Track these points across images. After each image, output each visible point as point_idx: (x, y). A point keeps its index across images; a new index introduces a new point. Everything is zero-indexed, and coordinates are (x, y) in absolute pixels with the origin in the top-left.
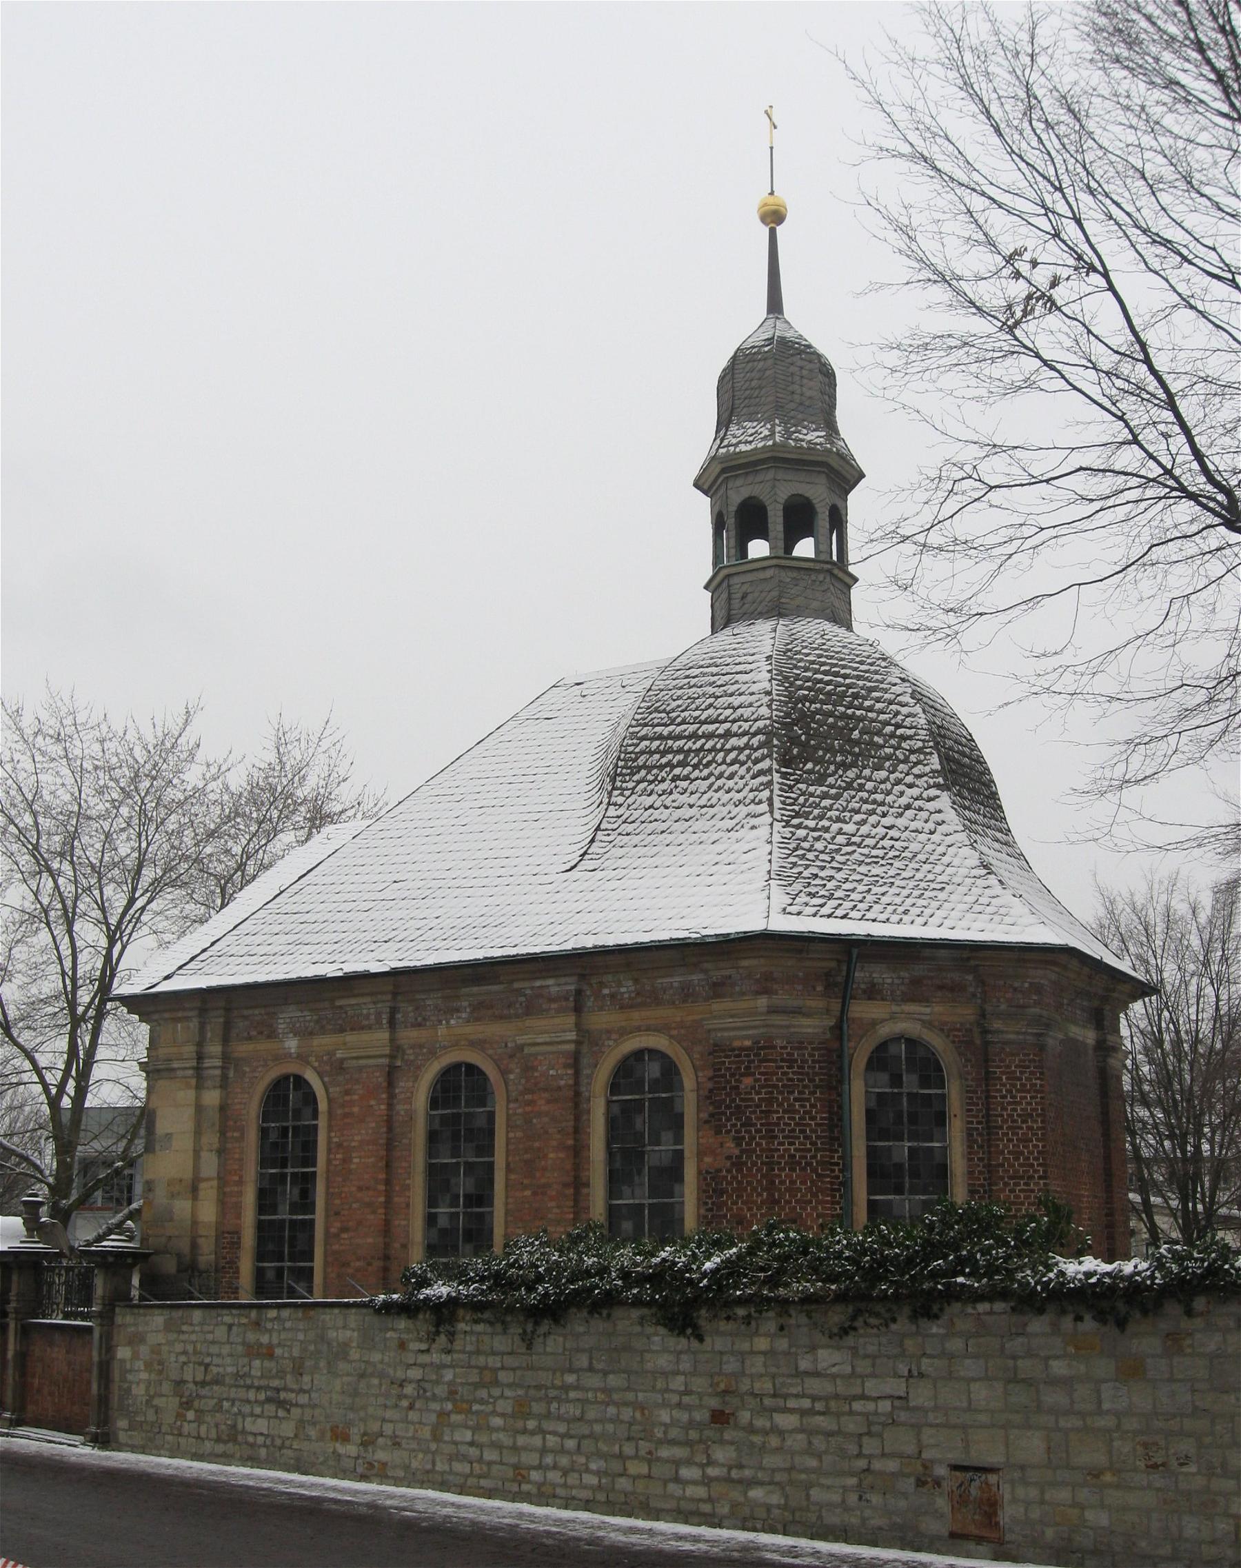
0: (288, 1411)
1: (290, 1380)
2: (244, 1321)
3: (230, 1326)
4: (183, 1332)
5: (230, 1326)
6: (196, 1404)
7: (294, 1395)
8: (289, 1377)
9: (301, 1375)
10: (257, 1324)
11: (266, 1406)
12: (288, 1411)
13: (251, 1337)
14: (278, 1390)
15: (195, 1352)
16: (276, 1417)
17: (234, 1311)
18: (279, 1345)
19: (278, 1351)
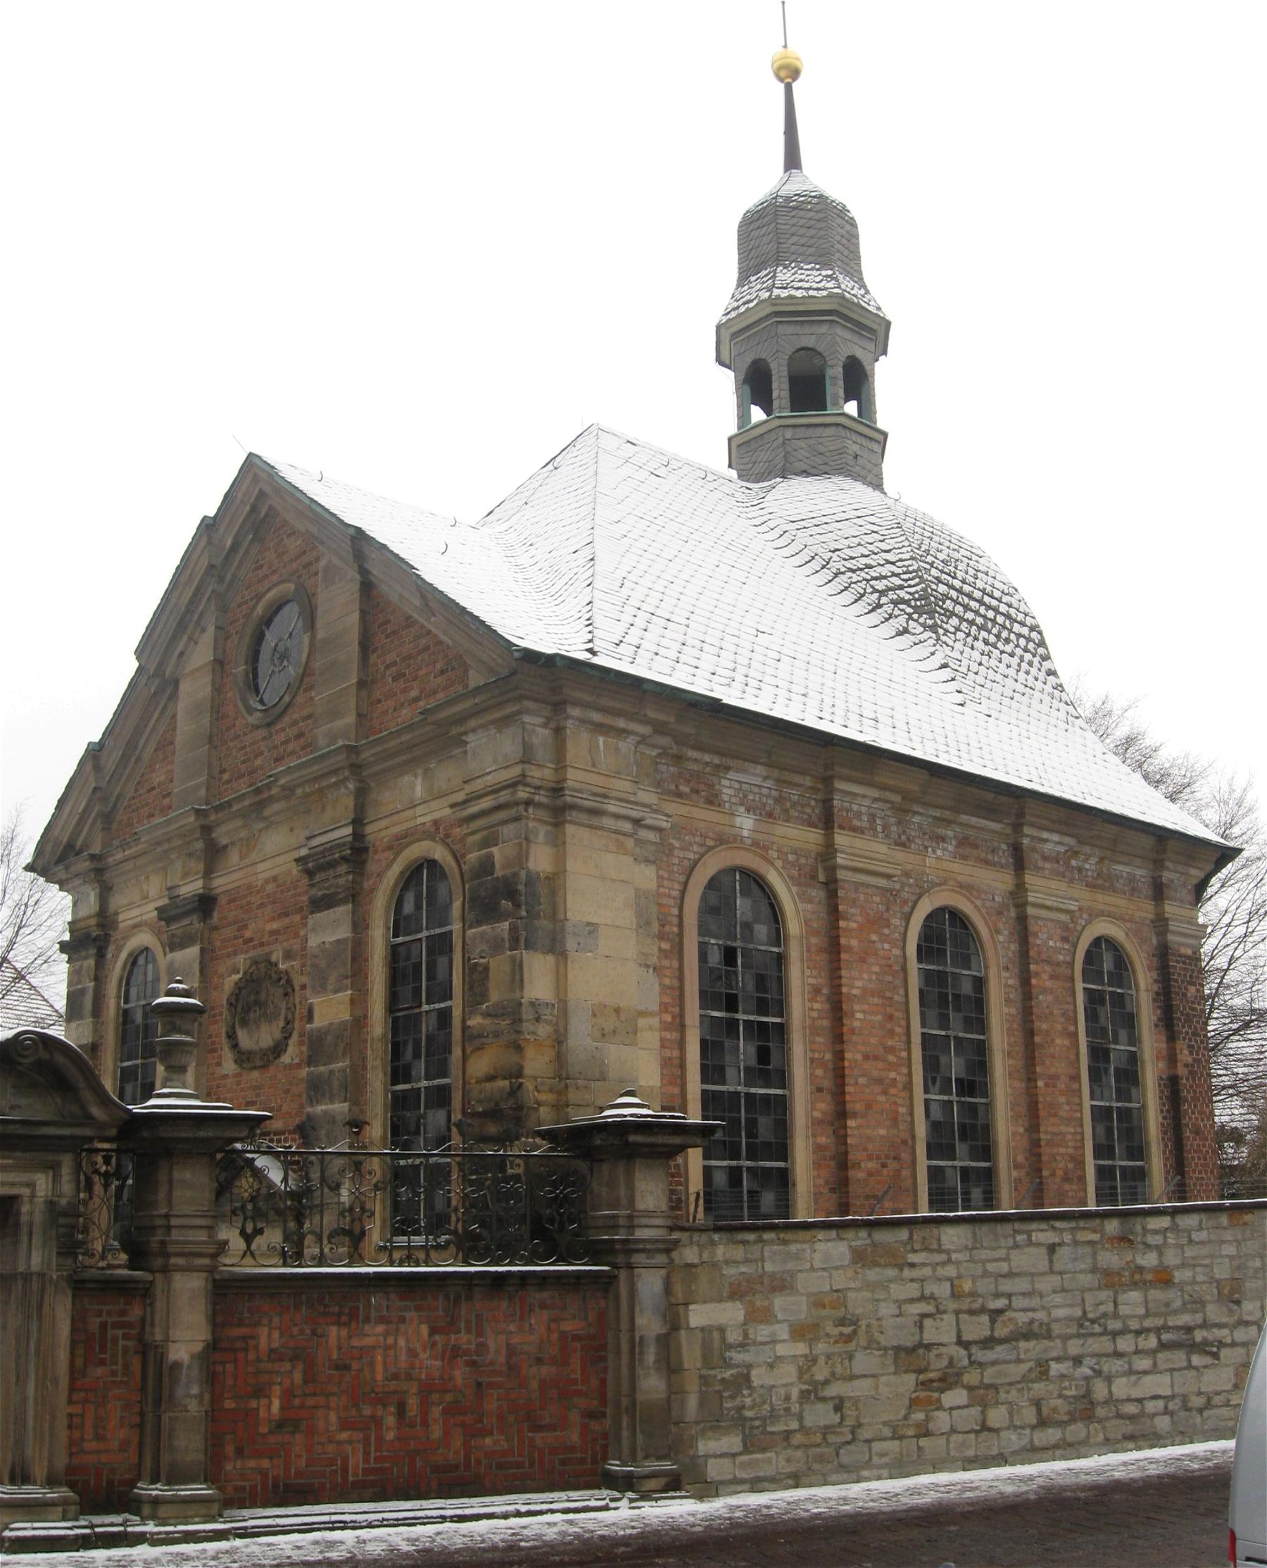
0: (1215, 1356)
1: (1214, 1312)
2: (1096, 1237)
3: (1052, 1248)
4: (912, 1265)
5: (1052, 1248)
6: (972, 1377)
7: (1226, 1332)
8: (1210, 1307)
9: (1238, 1302)
10: (1124, 1240)
11: (1160, 1356)
12: (1215, 1356)
13: (1111, 1259)
14: (1189, 1329)
15: (955, 1295)
16: (1190, 1366)
17: (1058, 1224)
18: (1183, 1265)
19: (1179, 1276)
